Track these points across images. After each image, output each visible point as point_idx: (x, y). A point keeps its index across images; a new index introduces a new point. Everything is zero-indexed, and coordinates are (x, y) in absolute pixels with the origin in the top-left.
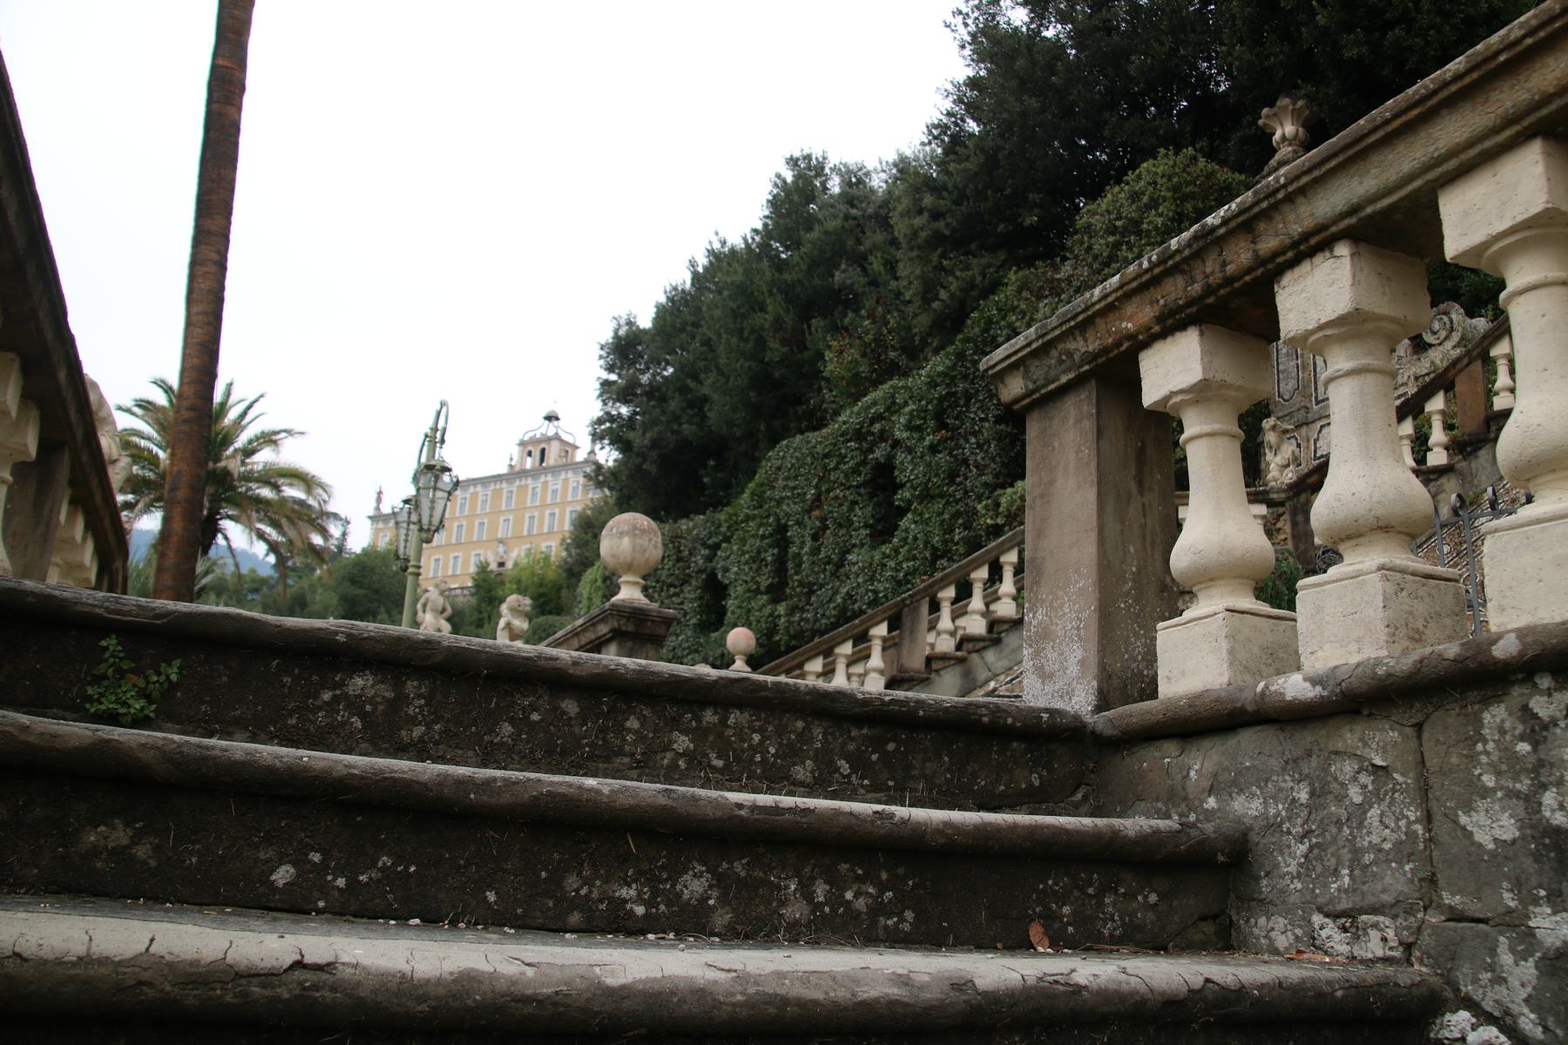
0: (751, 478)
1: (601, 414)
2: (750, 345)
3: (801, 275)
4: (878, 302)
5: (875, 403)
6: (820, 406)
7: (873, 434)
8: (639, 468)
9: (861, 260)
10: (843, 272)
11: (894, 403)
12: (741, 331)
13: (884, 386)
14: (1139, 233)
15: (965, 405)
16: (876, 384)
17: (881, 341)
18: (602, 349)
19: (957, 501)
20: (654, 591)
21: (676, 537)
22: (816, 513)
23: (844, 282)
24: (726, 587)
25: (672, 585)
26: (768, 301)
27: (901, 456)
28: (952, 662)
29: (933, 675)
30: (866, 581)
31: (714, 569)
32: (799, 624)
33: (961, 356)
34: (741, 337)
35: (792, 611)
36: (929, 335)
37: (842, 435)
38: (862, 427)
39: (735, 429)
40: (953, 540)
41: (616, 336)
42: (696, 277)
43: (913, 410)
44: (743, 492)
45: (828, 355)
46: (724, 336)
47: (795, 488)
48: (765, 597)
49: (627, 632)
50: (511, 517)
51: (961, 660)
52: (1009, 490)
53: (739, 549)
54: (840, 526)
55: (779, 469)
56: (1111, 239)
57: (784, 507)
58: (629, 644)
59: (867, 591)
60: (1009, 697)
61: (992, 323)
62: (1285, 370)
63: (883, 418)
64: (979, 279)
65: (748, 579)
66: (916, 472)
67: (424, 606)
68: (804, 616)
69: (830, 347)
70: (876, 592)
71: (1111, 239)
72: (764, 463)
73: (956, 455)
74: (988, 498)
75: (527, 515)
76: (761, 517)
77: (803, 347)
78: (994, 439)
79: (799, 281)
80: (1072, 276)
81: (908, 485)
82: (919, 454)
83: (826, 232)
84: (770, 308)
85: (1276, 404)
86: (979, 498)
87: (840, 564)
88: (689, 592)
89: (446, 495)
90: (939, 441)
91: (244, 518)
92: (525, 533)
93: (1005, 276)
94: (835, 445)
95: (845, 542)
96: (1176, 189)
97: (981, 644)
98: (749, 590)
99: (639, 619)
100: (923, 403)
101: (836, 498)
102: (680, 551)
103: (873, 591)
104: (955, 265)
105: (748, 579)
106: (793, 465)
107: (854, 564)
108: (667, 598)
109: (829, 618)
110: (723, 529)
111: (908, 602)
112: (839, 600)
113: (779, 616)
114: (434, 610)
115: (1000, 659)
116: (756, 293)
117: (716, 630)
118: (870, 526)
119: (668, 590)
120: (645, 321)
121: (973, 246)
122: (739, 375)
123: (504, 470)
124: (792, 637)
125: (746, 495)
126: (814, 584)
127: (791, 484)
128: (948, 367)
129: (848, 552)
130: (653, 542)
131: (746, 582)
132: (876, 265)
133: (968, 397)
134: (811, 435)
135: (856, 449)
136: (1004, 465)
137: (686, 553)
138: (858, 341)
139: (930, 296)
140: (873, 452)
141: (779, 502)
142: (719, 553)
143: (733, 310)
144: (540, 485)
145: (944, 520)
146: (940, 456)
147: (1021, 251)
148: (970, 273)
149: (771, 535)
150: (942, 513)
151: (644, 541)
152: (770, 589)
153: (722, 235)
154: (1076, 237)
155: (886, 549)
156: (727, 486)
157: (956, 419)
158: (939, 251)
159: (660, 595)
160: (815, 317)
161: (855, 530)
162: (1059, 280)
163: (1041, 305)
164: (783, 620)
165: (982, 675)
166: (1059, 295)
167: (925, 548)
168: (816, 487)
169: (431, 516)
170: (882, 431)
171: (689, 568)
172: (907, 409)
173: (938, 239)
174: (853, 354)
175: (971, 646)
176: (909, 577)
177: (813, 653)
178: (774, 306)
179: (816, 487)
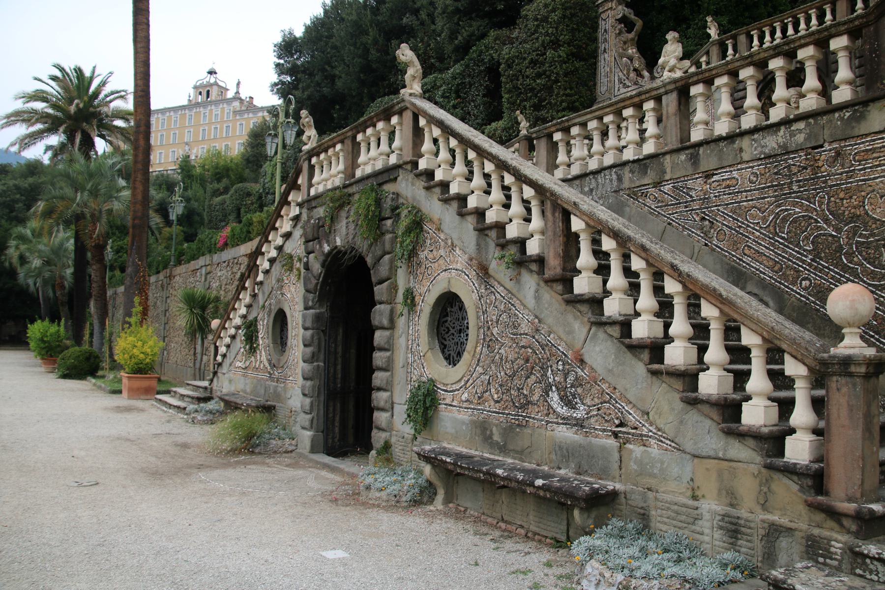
1: (277, 81)
2: (360, 52)
9: (416, 12)
11: (435, 85)
14: (547, 22)
33: (467, 66)
41: (284, 40)
42: (326, 12)
50: (192, 130)
52: (488, 127)
61: (482, 52)
71: (535, 23)
75: (201, 129)
79: (386, 21)
84: (371, 34)
93: (488, 32)
96: (563, 5)
120: (299, 32)
121: (473, 15)
123: (185, 103)
132: (423, 15)
133: (471, 86)
136: (486, 115)
139: (453, 37)
143: (351, 33)
158: (458, 16)
162: (513, 38)
172: (442, 88)
173: (457, 11)
178: (373, 33)
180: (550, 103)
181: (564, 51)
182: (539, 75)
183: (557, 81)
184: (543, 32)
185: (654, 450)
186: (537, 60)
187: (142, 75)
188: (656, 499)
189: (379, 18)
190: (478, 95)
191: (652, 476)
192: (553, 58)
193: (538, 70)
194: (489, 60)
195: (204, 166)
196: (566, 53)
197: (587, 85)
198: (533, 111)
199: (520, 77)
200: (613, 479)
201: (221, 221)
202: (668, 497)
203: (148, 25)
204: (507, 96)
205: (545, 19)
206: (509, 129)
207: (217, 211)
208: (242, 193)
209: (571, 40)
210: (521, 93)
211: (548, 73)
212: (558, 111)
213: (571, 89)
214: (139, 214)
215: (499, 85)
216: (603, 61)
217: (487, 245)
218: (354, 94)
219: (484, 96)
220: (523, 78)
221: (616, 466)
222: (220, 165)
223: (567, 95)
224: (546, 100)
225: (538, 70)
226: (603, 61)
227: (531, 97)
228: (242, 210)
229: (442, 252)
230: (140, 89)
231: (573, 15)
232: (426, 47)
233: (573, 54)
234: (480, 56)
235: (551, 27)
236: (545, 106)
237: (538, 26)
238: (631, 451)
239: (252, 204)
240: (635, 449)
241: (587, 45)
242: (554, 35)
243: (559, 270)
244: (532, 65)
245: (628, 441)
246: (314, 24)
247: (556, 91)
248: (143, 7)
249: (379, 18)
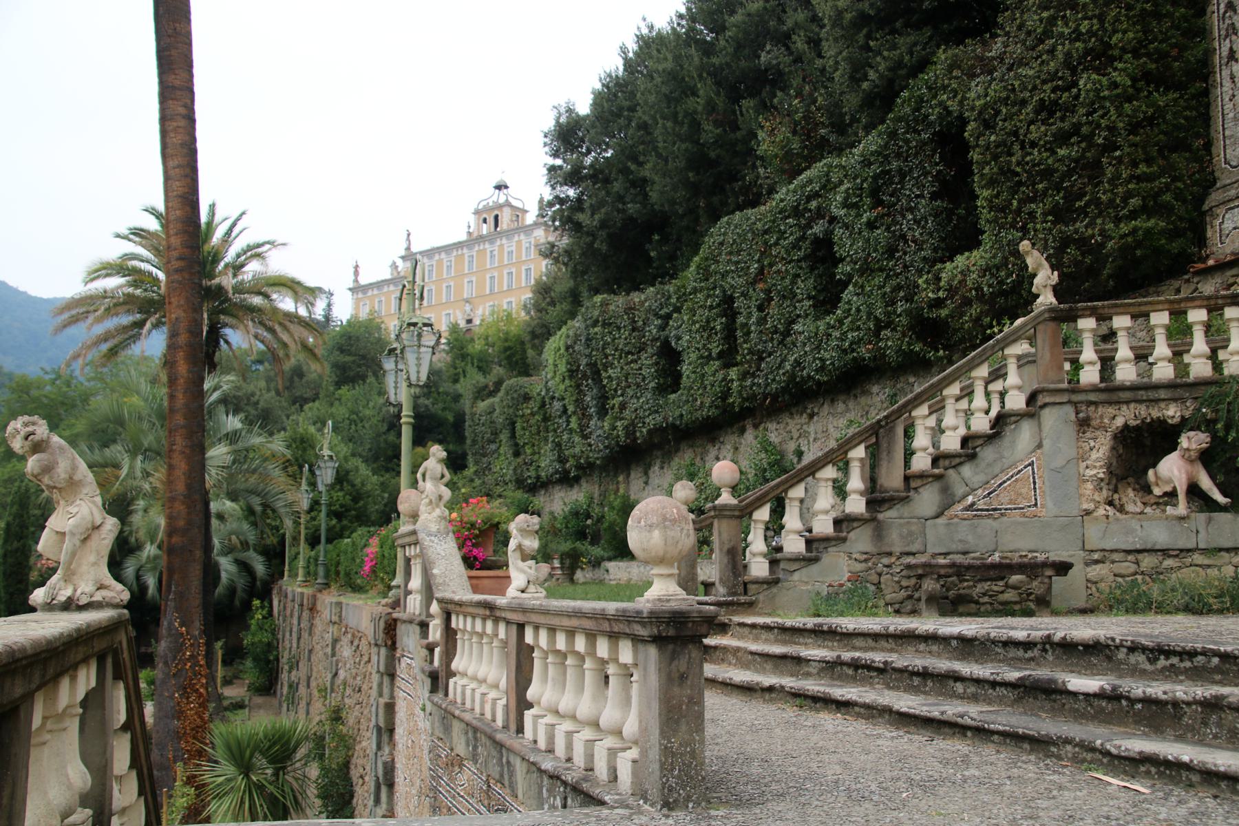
0: (696, 253)
2: (685, 128)
3: (728, 59)
4: (804, 79)
5: (810, 181)
6: (756, 182)
7: (810, 210)
8: (591, 245)
9: (784, 39)
10: (768, 52)
11: (828, 181)
12: (675, 115)
13: (818, 164)
15: (899, 183)
16: (811, 160)
17: (810, 118)
18: (546, 136)
19: (897, 275)
20: (614, 359)
21: (631, 309)
22: (760, 286)
23: (770, 63)
24: (680, 353)
25: (629, 353)
26: (699, 86)
27: (838, 232)
28: (930, 479)
29: (912, 493)
30: (812, 350)
31: (667, 337)
32: (751, 389)
33: (893, 135)
34: (676, 122)
35: (744, 376)
36: (857, 112)
37: (780, 213)
38: (799, 204)
39: (677, 207)
40: (895, 312)
42: (628, 64)
43: (849, 189)
44: (688, 266)
45: (761, 135)
46: (660, 121)
47: (737, 263)
48: (717, 363)
49: (667, 637)
50: (474, 279)
51: (939, 477)
53: (689, 319)
54: (784, 297)
55: (722, 244)
56: (1045, 14)
57: (729, 280)
58: (671, 647)
59: (815, 359)
60: (987, 510)
61: (922, 101)
62: (1232, 136)
63: (820, 196)
64: (907, 58)
65: (700, 346)
66: (855, 247)
67: (424, 475)
68: (756, 381)
69: (762, 127)
70: (822, 360)
71: (1045, 14)
72: (706, 239)
73: (894, 231)
74: (928, 272)
75: (488, 276)
76: (708, 289)
77: (735, 127)
78: (930, 215)
79: (727, 64)
80: (1005, 53)
81: (848, 259)
82: (856, 230)
83: (749, 15)
84: (701, 92)
85: (1223, 170)
86: (920, 272)
87: (787, 333)
88: (646, 359)
89: (431, 350)
90: (876, 217)
91: (242, 327)
92: (488, 292)
93: (934, 53)
94: (774, 221)
95: (790, 313)
97: (957, 460)
98: (702, 357)
99: (681, 623)
100: (858, 181)
101: (779, 272)
102: (635, 322)
103: (820, 359)
104: (882, 45)
105: (700, 346)
106: (734, 241)
107: (800, 333)
108: (626, 364)
109: (780, 383)
110: (673, 300)
111: (883, 423)
112: (789, 367)
113: (732, 380)
114: (432, 478)
115: (977, 474)
116: (687, 79)
117: (675, 392)
118: (813, 298)
119: (626, 357)
120: (584, 108)
121: (898, 24)
122: (677, 157)
123: (463, 237)
124: (745, 400)
125: (693, 268)
126: (763, 352)
127: (734, 259)
128: (880, 146)
129: (793, 322)
130: (685, 531)
131: (698, 349)
132: (799, 44)
133: (903, 174)
134: (750, 211)
135: (795, 225)
136: (942, 240)
137: (641, 323)
138: (787, 118)
140: (812, 228)
141: (724, 275)
142: (671, 323)
143: (665, 95)
144: (497, 248)
145: (885, 293)
146: (879, 231)
147: (945, 26)
148: (898, 51)
149: (718, 305)
150: (884, 287)
151: (674, 533)
152: (721, 355)
153: (649, 20)
154: (1006, 14)
155: (830, 319)
156: (672, 258)
157: (891, 196)
158: (864, 31)
159: (619, 362)
160: (745, 98)
161: (799, 301)
162: (993, 58)
163: (973, 84)
164: (735, 384)
165: (960, 490)
166: (990, 73)
167: (868, 318)
168: (758, 261)
169: (418, 372)
170: (819, 208)
171: (644, 337)
172: (843, 188)
173: (863, 20)
174: (784, 132)
175: (947, 462)
176: (854, 346)
177: (795, 480)
178: (705, 89)
179: (758, 261)
180: (1096, 202)
181: (1124, 70)
182: (1063, 138)
183: (1110, 147)
184: (1067, 31)
186: (1055, 103)
187: (179, 226)
189: (715, 60)
190: (921, 196)
192: (1097, 91)
193: (1059, 124)
194: (940, 116)
195: (487, 338)
196: (1128, 75)
197: (1188, 148)
199: (1016, 147)
201: (491, 442)
203: (191, 120)
204: (986, 193)
206: (998, 268)
207: (483, 425)
208: (515, 395)
209: (1140, 42)
210: (1020, 184)
211: (1085, 130)
212: (1117, 220)
213: (1149, 161)
214: (181, 523)
215: (966, 170)
216: (1227, 84)
218: (680, 211)
219: (934, 196)
220: (1023, 148)
222: (512, 334)
223: (1139, 179)
224: (1085, 194)
225: (1059, 124)
226: (1227, 84)
227: (1047, 189)
228: (518, 426)
230: (175, 254)
232: (809, 105)
233: (1147, 76)
234: (918, 109)
235: (1085, 18)
236: (1083, 211)
237: (1052, 21)
239: (533, 414)
241: (1182, 48)
242: (1095, 34)
244: (1044, 115)
246: (608, 87)
247: (1109, 172)
248: (177, 83)
249: (715, 60)
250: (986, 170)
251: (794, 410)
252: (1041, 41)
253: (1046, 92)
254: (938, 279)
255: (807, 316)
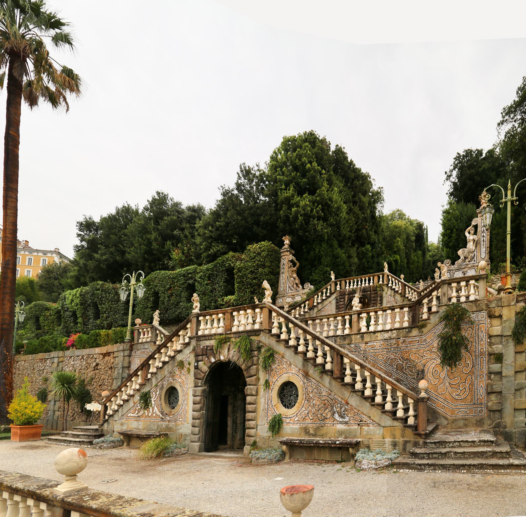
14: (260, 255)
27: (196, 284)
33: (215, 266)
86: (219, 298)
87: (177, 305)
107: (182, 306)
133: (217, 276)
166: (242, 261)
180: (259, 292)
182: (255, 279)
185: (371, 427)
188: (372, 441)
190: (221, 281)
191: (371, 435)
192: (262, 272)
198: (250, 294)
200: (358, 438)
202: (376, 440)
205: (259, 254)
206: (238, 300)
210: (245, 285)
217: (308, 365)
219: (224, 282)
221: (359, 434)
227: (249, 287)
229: (284, 366)
231: (271, 255)
234: (223, 263)
236: (256, 293)
237: (255, 256)
238: (364, 429)
240: (366, 428)
243: (339, 375)
245: (363, 426)
250: (238, 280)
251: (174, 325)
252: (252, 259)
253: (253, 269)
254: (223, 300)
255: (184, 302)
